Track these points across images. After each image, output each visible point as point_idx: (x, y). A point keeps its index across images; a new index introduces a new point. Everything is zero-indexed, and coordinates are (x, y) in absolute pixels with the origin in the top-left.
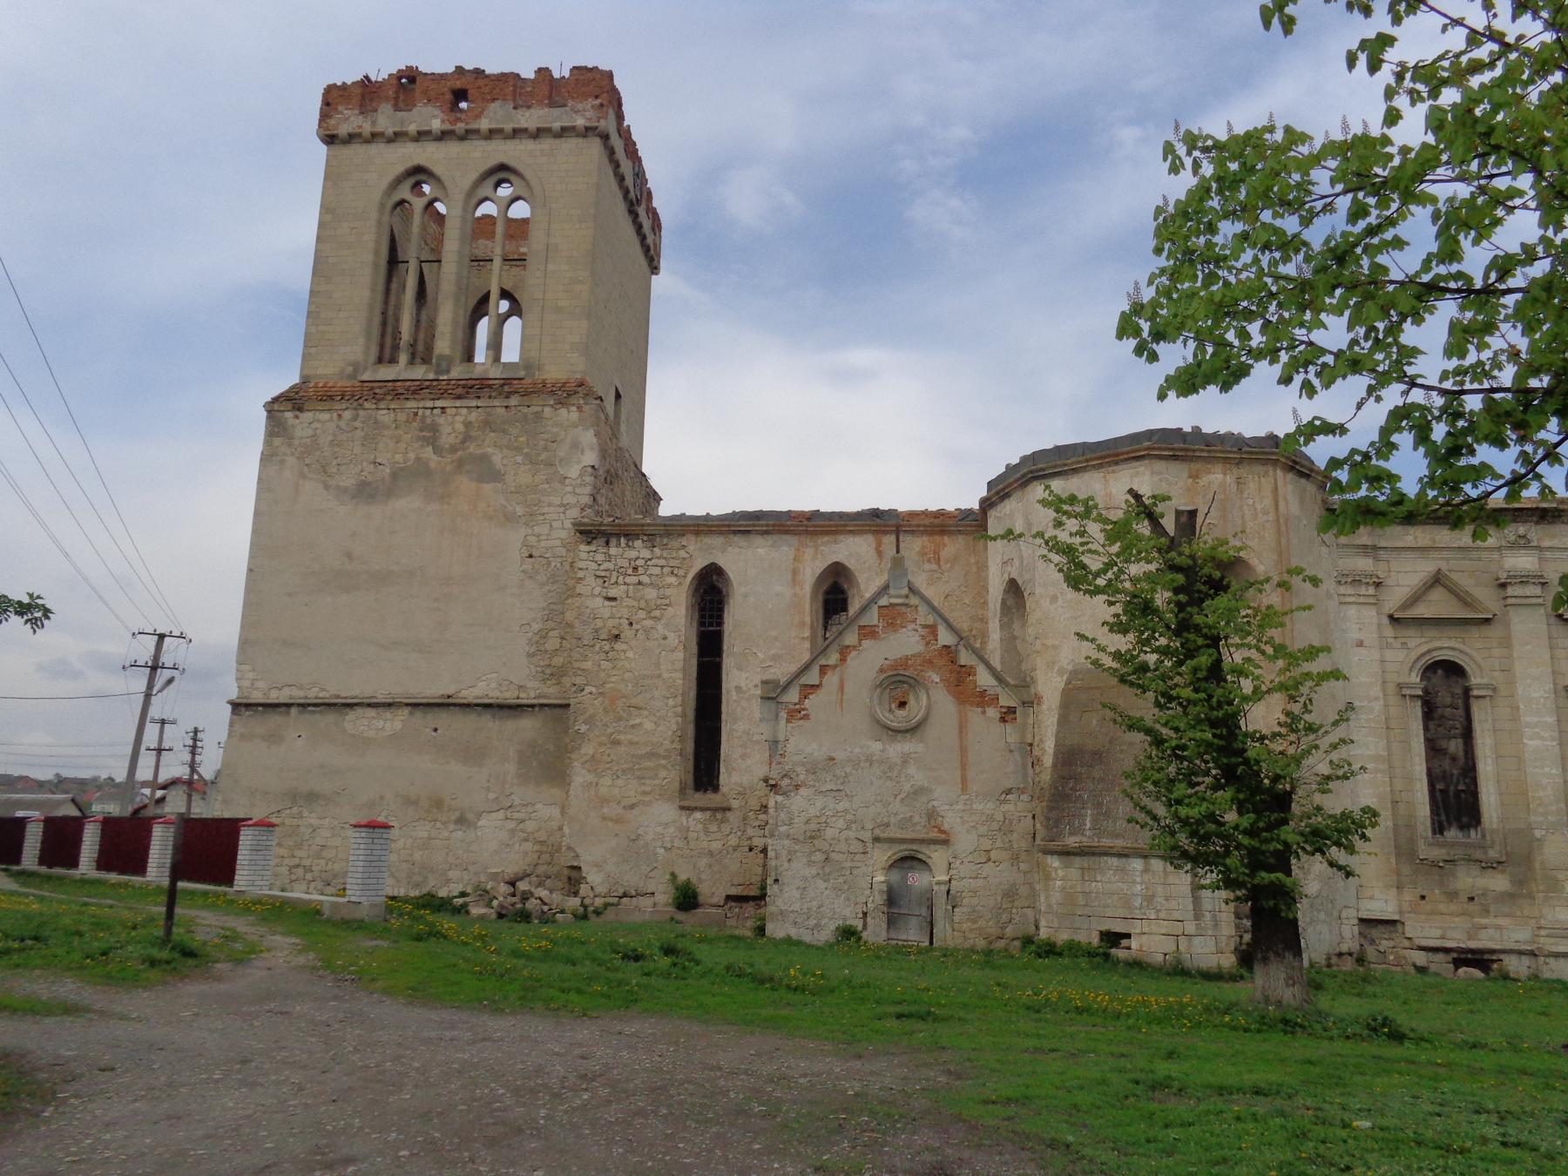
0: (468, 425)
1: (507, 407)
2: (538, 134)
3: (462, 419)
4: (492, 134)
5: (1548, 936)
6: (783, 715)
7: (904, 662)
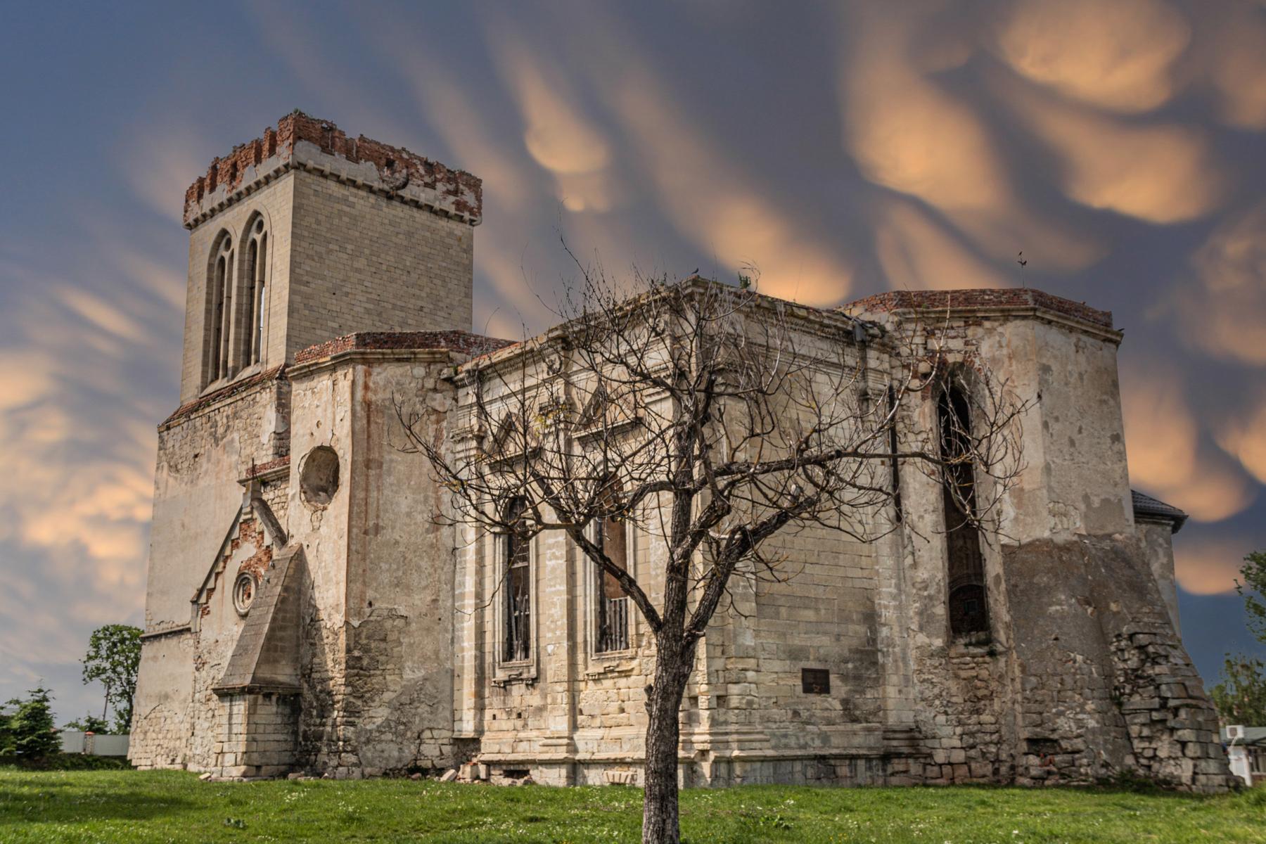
0: (228, 417)
1: (242, 399)
2: (268, 180)
4: (249, 191)
5: (544, 745)
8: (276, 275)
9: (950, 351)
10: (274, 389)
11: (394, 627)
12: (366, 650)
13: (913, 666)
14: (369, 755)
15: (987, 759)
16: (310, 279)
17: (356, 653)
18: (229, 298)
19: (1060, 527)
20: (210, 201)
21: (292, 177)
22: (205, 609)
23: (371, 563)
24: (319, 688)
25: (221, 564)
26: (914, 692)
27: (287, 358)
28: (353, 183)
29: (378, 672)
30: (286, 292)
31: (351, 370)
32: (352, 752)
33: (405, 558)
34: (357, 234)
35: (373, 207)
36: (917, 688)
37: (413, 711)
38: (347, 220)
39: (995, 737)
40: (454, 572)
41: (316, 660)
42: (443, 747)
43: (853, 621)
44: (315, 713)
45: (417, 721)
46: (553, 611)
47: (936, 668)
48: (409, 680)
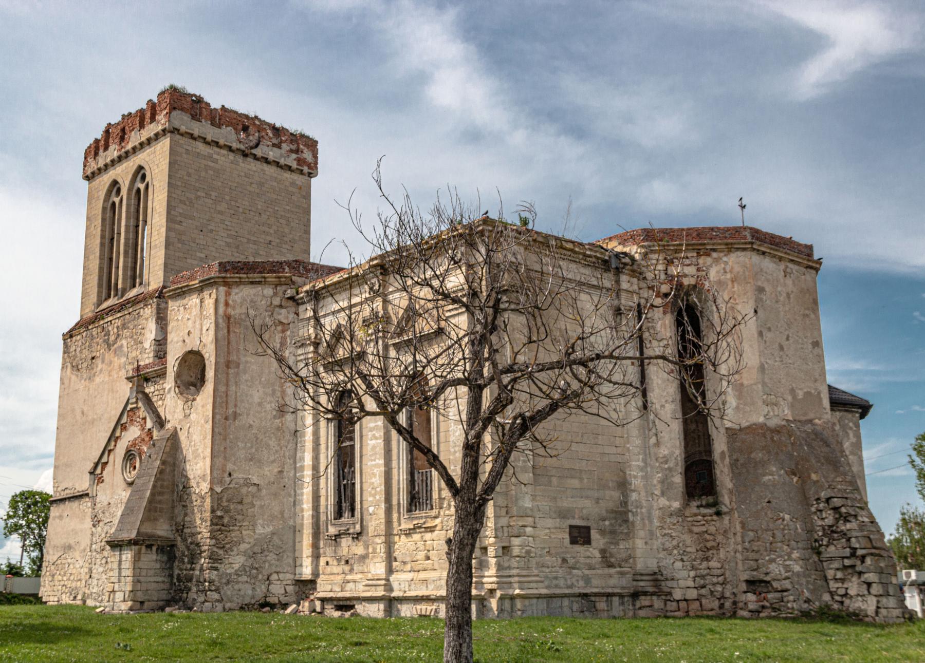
0: (118, 327)
2: (149, 141)
3: (116, 325)
5: (366, 586)
6: (96, 481)
7: (134, 444)
8: (156, 216)
9: (685, 276)
10: (154, 306)
11: (248, 492)
12: (227, 511)
13: (656, 523)
14: (229, 593)
15: (715, 596)
16: (183, 219)
17: (219, 513)
18: (119, 234)
19: (772, 414)
20: (104, 158)
21: (169, 139)
22: (100, 478)
23: (231, 442)
24: (189, 540)
25: (113, 443)
26: (657, 544)
27: (164, 281)
28: (217, 144)
29: (236, 528)
30: (164, 230)
31: (215, 291)
32: (215, 590)
33: (257, 439)
34: (220, 184)
35: (232, 163)
36: (659, 541)
37: (264, 558)
38: (211, 172)
39: (721, 579)
40: (296, 449)
41: (187, 519)
42: (287, 587)
43: (609, 488)
44: (186, 560)
45: (267, 567)
46: (373, 480)
47: (674, 524)
48: (260, 535)
